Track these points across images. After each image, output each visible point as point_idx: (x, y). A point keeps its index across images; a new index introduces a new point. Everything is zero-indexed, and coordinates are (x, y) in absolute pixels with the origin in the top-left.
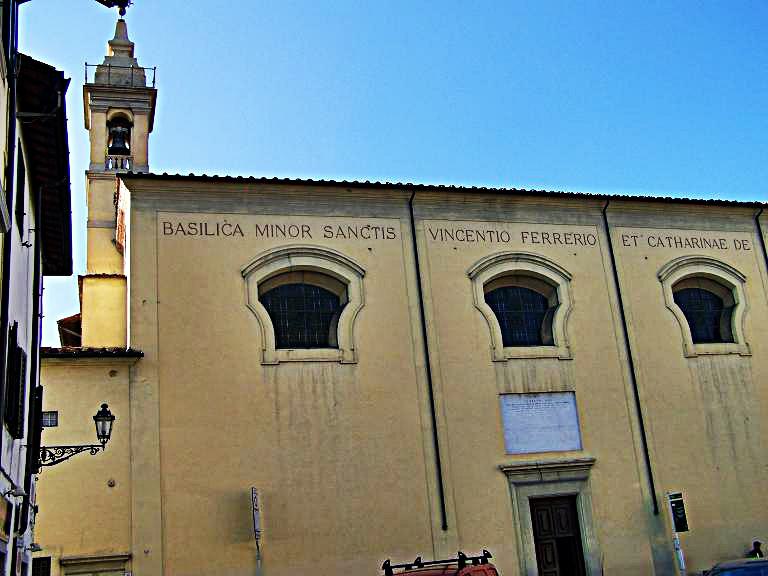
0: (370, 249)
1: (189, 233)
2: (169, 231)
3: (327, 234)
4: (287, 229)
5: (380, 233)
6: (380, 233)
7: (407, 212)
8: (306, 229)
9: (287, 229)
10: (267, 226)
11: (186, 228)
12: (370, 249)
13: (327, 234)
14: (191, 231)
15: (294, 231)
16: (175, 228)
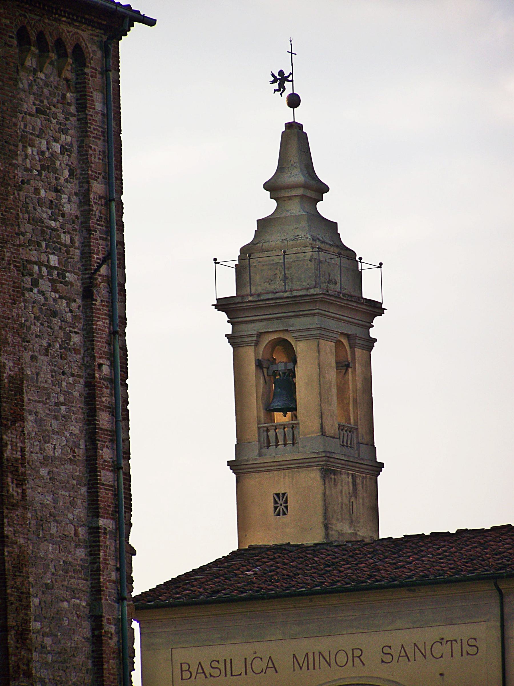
0: (441, 675)
1: (211, 676)
2: (186, 675)
3: (388, 658)
4: (333, 657)
5: (456, 647)
6: (456, 647)
7: (497, 611)
8: (357, 653)
9: (333, 657)
10: (307, 654)
11: (208, 670)
12: (441, 675)
13: (388, 658)
14: (216, 673)
15: (342, 659)
16: (193, 670)
